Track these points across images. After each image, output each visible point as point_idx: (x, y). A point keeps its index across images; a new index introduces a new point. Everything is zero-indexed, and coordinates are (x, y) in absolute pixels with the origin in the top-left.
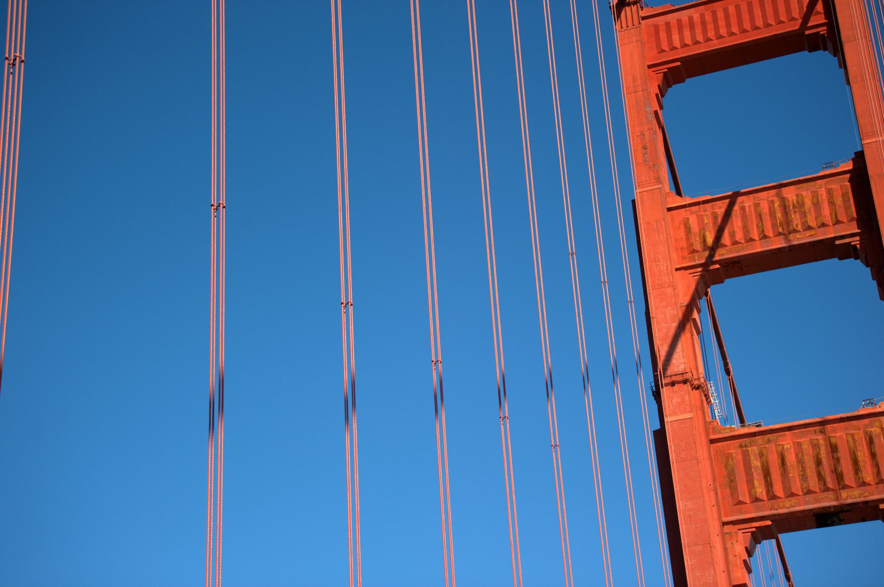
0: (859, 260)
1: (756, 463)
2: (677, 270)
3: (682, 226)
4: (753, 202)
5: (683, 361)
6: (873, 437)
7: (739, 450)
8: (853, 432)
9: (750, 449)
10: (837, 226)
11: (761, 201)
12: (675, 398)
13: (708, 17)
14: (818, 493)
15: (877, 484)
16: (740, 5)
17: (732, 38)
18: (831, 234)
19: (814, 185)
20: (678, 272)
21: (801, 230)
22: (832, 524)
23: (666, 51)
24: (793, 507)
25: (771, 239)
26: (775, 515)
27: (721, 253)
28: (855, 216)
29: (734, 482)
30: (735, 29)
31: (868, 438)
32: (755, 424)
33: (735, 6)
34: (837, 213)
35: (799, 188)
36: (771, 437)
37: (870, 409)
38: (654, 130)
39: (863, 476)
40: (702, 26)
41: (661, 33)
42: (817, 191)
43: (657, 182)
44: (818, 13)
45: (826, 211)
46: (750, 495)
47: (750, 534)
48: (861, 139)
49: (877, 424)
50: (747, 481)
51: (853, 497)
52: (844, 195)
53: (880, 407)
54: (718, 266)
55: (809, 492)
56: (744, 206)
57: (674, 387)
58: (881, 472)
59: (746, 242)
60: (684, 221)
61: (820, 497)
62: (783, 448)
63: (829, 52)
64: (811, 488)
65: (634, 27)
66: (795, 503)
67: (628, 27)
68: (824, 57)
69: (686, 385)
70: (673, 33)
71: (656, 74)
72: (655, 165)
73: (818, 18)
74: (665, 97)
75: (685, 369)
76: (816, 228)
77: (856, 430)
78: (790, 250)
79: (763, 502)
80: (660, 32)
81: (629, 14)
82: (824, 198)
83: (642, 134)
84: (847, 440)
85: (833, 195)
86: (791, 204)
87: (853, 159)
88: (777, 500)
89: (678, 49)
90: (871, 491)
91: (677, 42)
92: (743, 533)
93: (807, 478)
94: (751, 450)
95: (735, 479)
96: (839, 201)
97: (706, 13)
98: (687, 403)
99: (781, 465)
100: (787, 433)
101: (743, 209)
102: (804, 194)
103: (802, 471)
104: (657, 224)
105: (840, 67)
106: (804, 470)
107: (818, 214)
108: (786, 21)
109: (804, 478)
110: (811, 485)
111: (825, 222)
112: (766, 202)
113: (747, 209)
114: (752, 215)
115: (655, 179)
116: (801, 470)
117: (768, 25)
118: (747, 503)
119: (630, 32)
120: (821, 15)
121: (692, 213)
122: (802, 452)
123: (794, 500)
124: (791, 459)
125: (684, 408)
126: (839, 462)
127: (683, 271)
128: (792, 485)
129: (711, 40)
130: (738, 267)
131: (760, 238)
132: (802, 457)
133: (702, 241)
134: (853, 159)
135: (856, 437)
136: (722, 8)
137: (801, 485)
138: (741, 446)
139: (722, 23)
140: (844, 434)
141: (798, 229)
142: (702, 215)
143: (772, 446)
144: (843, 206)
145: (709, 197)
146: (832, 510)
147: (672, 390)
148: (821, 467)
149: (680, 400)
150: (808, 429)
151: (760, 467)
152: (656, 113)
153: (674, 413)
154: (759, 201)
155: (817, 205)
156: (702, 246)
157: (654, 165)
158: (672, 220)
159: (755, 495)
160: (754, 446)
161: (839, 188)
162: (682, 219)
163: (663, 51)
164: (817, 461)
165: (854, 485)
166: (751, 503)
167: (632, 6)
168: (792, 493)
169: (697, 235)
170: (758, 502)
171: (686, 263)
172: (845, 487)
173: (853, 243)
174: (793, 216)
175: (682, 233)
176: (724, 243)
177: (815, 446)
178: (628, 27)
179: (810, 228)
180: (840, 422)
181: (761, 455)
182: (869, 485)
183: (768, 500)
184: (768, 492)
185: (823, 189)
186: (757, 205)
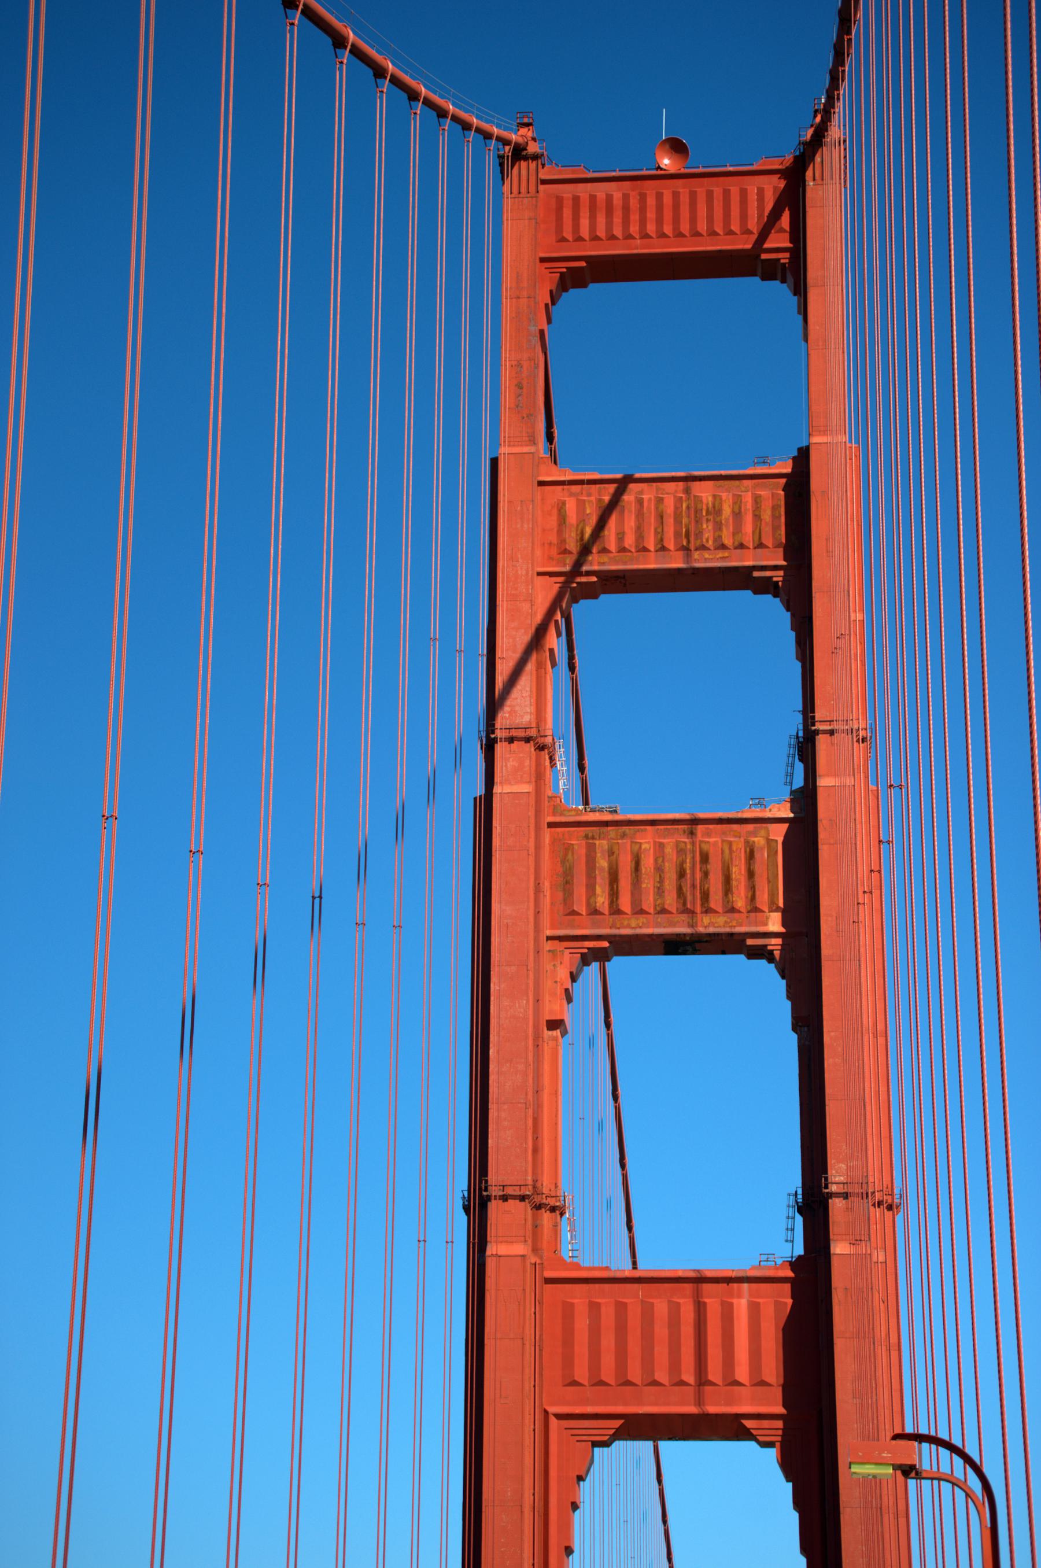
0: (778, 599)
1: (603, 863)
2: (539, 574)
3: (555, 512)
4: (655, 495)
5: (529, 711)
6: (755, 850)
7: (584, 842)
8: (732, 839)
9: (597, 842)
10: (759, 551)
11: (666, 496)
12: (511, 760)
13: (634, 203)
14: (673, 913)
15: (749, 912)
16: (679, 192)
17: (663, 241)
18: (749, 561)
19: (739, 486)
20: (539, 577)
21: (712, 548)
22: (685, 953)
23: (568, 241)
24: (640, 927)
25: (671, 553)
26: (615, 936)
27: (602, 561)
28: (784, 541)
29: (569, 883)
30: (668, 229)
31: (748, 850)
32: (609, 808)
33: (673, 192)
34: (762, 533)
35: (719, 487)
36: (627, 831)
37: (757, 811)
38: (536, 362)
39: (734, 899)
40: (623, 213)
41: (565, 210)
42: (740, 496)
43: (530, 440)
44: (782, 230)
45: (748, 527)
46: (588, 904)
47: (579, 955)
48: (809, 435)
49: (763, 833)
50: (587, 885)
51: (716, 925)
52: (774, 508)
53: (770, 810)
54: (594, 579)
55: (663, 911)
56: (643, 499)
57: (512, 744)
58: (757, 897)
59: (637, 551)
60: (558, 504)
61: (676, 920)
62: (640, 847)
63: (788, 286)
64: (666, 907)
65: (528, 195)
66: (643, 923)
67: (520, 193)
68: (780, 291)
69: (528, 745)
70: (581, 214)
71: (550, 273)
72: (531, 415)
73: (779, 240)
74: (557, 305)
75: (530, 722)
76: (732, 548)
77: (735, 836)
78: (693, 574)
79: (602, 916)
80: (564, 209)
81: (524, 172)
82: (748, 507)
83: (519, 365)
84: (722, 849)
85: (761, 506)
86: (705, 507)
87: (794, 458)
88: (622, 916)
89: (585, 241)
90: (740, 921)
91: (585, 232)
92: (570, 953)
93: (663, 892)
94: (599, 844)
95: (572, 881)
96: (767, 516)
97: (632, 194)
98: (526, 769)
99: (633, 870)
100: (649, 828)
101: (640, 502)
102: (724, 495)
103: (659, 882)
104: (521, 506)
105: (799, 313)
106: (661, 881)
107: (737, 530)
108: (738, 232)
109: (660, 891)
110: (668, 902)
111: (745, 543)
112: (672, 499)
113: (646, 504)
114: (651, 513)
115: (528, 436)
116: (658, 880)
117: (713, 233)
118: (582, 915)
119: (522, 201)
120: (786, 234)
121: (571, 495)
122: (663, 857)
123: (642, 919)
124: (648, 864)
125: (521, 777)
126: (707, 877)
127: (548, 577)
128: (643, 899)
129: (634, 238)
130: (620, 582)
131: (657, 548)
132: (662, 864)
133: (578, 538)
134: (794, 458)
135: (734, 848)
136: (654, 192)
137: (655, 900)
138: (586, 837)
139: (651, 215)
140: (718, 840)
141: (708, 546)
142: (584, 500)
143: (627, 842)
144: (771, 522)
145: (597, 476)
146: (688, 938)
147: (508, 749)
148: (683, 880)
149: (517, 765)
150: (677, 827)
151: (607, 869)
152: (542, 333)
153: (508, 782)
154: (663, 494)
155: (737, 515)
156: (577, 546)
157: (529, 415)
158: (543, 499)
159: (594, 905)
160: (603, 839)
161: (770, 496)
162: (556, 500)
163: (563, 240)
164: (680, 872)
165: (720, 909)
166: (588, 915)
167: (530, 161)
168: (642, 909)
169: (574, 529)
170: (597, 915)
171: (553, 566)
172: (708, 911)
173: (775, 579)
174: (705, 526)
175: (553, 522)
176: (608, 548)
177: (680, 851)
178: (520, 193)
179: (723, 547)
180: (717, 824)
181: (611, 853)
182: (740, 912)
183: (610, 914)
184: (611, 903)
185: (750, 493)
186: (660, 501)
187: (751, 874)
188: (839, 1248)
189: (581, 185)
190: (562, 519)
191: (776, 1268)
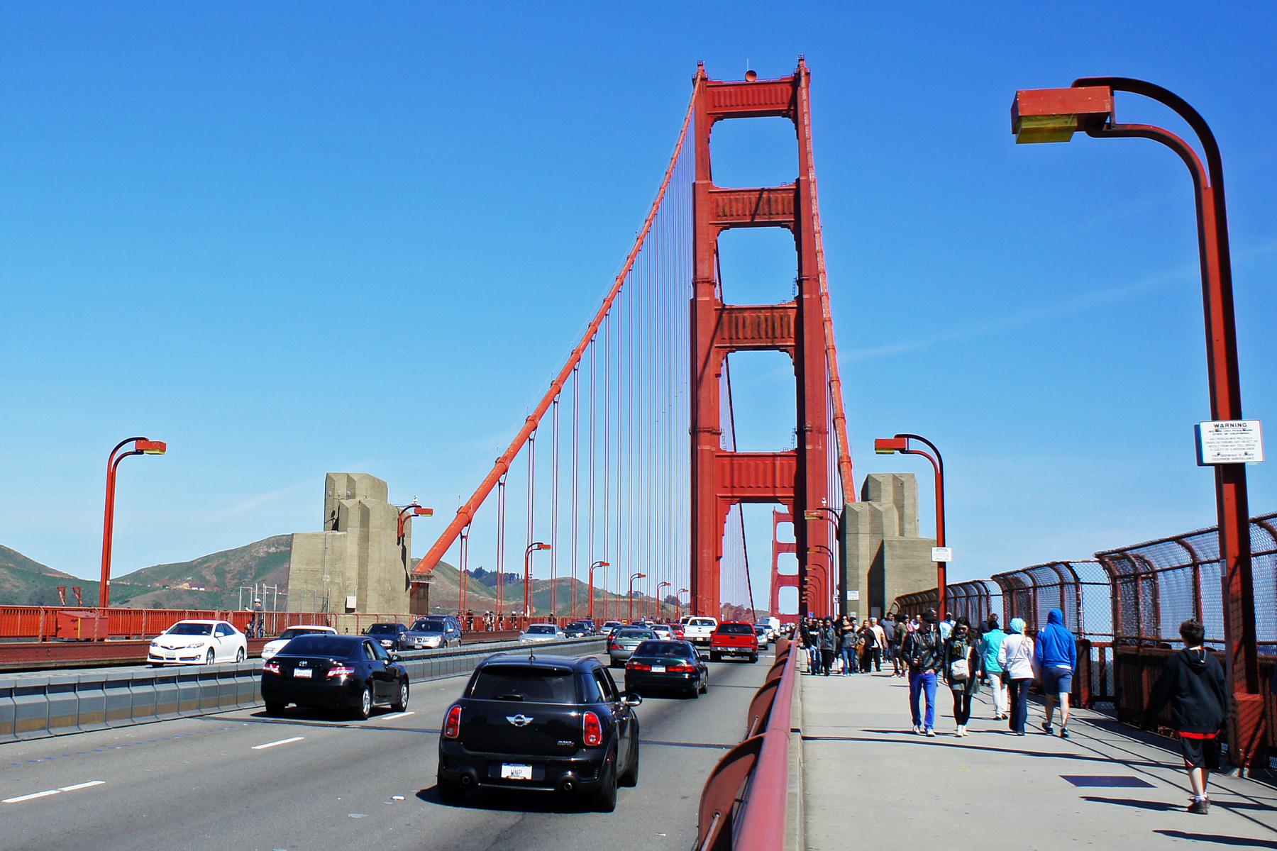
2: (711, 224)
13: (739, 94)
68: (788, 121)
124: (748, 322)
163: (715, 107)
187: (782, 325)
188: (808, 447)
189: (720, 88)
190: (717, 206)
191: (788, 452)
